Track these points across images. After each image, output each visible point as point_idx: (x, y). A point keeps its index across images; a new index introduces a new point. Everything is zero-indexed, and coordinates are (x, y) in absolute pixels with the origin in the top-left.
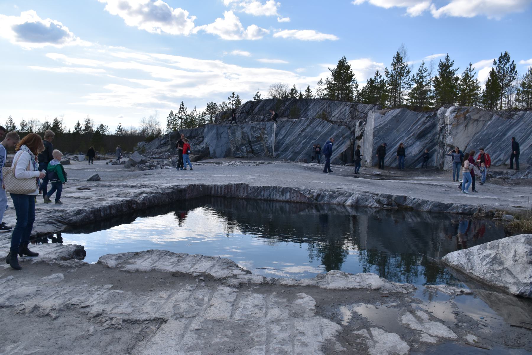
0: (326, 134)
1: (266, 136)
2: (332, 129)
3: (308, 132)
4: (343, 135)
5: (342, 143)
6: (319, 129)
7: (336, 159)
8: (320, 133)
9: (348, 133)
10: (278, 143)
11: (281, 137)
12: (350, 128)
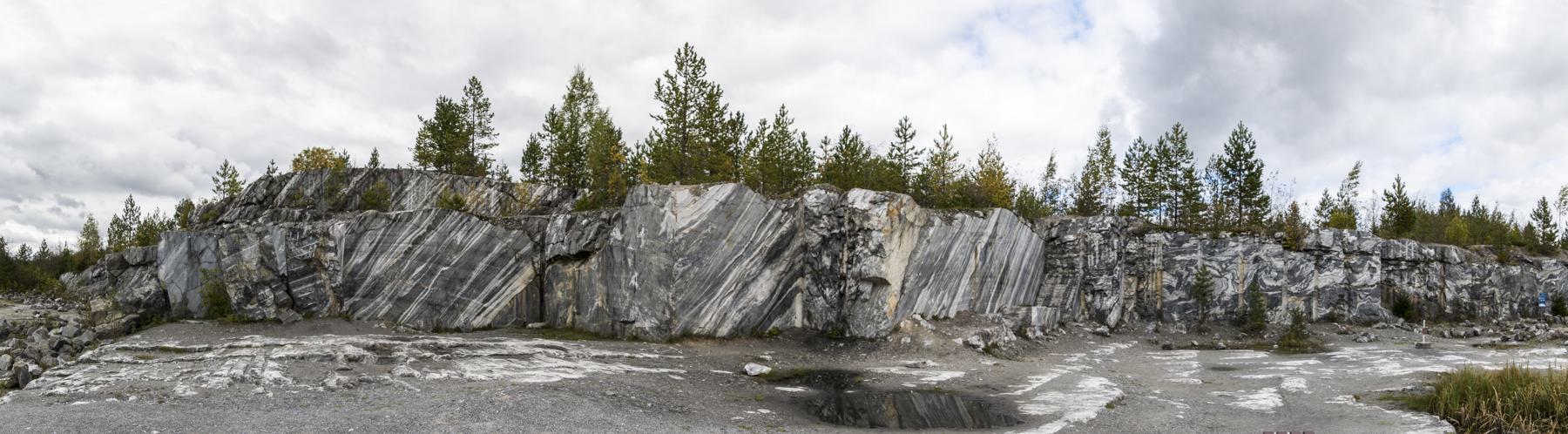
0: (477, 252)
1: (331, 255)
2: (491, 237)
3: (430, 245)
4: (517, 251)
5: (515, 272)
6: (459, 237)
7: (500, 312)
8: (461, 247)
9: (528, 247)
10: (353, 273)
11: (359, 260)
12: (531, 236)
